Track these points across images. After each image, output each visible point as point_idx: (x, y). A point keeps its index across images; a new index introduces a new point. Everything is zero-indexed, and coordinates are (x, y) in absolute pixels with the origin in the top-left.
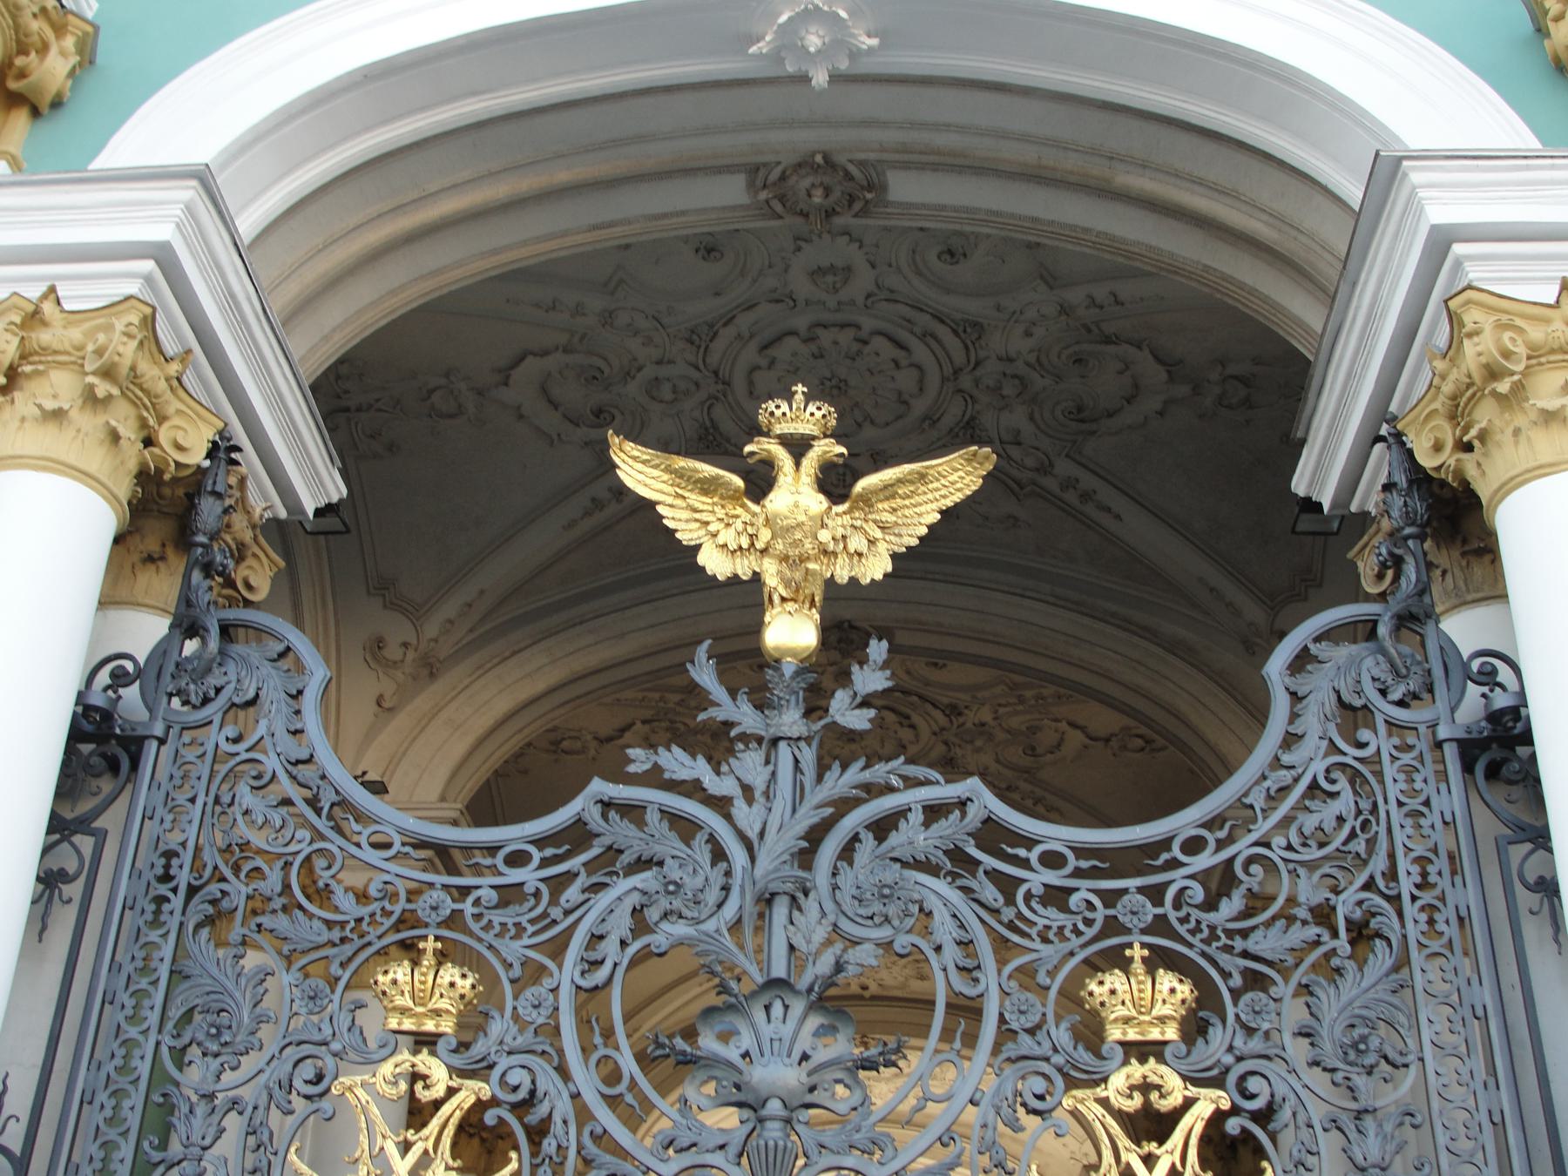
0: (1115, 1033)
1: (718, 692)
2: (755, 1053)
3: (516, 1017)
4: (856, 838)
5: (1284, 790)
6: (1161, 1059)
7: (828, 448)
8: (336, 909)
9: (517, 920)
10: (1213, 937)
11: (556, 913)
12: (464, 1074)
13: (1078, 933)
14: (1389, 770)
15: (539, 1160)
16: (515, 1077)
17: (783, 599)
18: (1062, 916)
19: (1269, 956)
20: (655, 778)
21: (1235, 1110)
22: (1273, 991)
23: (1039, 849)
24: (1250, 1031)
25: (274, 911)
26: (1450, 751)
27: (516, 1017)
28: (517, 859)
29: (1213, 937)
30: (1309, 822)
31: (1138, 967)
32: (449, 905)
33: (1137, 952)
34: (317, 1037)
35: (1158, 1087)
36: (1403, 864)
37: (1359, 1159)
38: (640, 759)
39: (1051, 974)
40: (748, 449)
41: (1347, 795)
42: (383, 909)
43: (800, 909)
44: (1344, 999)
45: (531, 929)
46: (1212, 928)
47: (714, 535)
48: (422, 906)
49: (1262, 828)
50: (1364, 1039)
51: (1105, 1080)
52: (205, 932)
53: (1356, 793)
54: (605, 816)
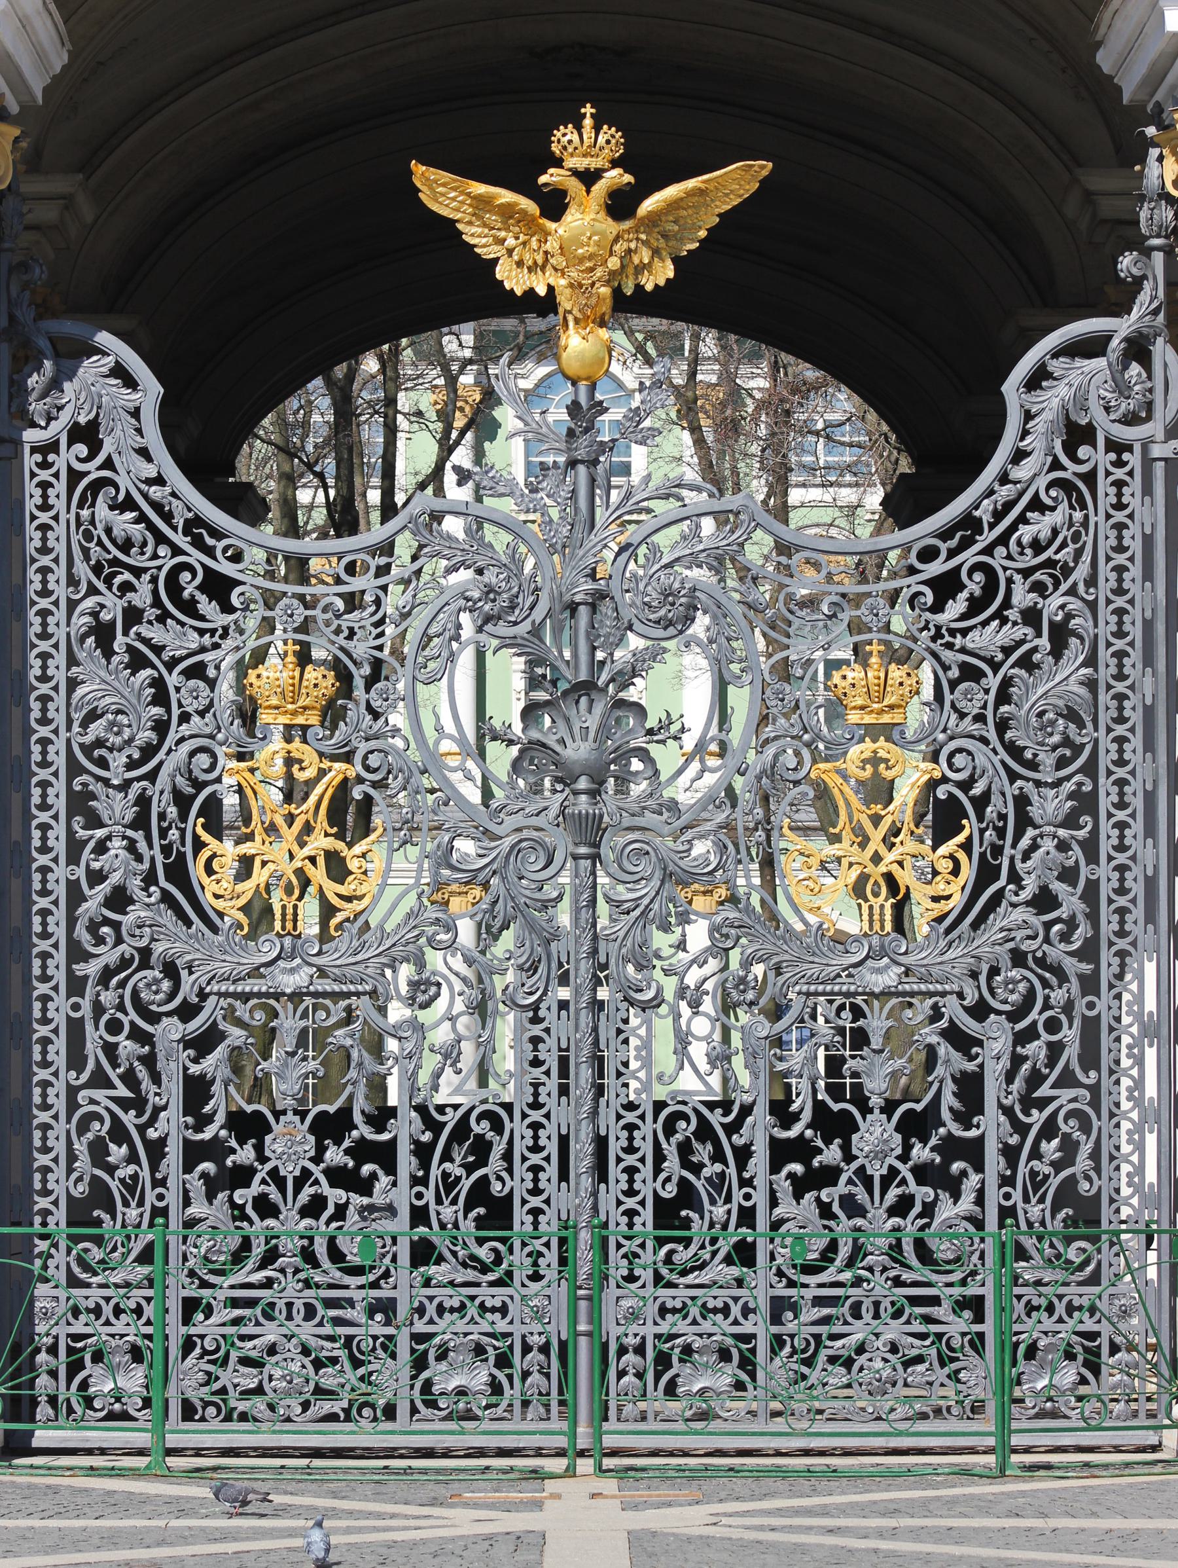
0: (854, 717)
2: (568, 741)
3: (369, 708)
5: (1009, 506)
7: (616, 177)
8: (203, 618)
10: (938, 636)
12: (334, 758)
14: (1102, 484)
16: (374, 761)
21: (945, 780)
22: (984, 681)
24: (962, 716)
26: (1159, 468)
30: (1026, 533)
32: (301, 613)
34: (208, 730)
36: (1104, 570)
37: (1038, 821)
40: (543, 179)
44: (1040, 691)
46: (938, 628)
47: (510, 252)
49: (987, 537)
50: (1052, 723)
52: (90, 641)
53: (1072, 507)
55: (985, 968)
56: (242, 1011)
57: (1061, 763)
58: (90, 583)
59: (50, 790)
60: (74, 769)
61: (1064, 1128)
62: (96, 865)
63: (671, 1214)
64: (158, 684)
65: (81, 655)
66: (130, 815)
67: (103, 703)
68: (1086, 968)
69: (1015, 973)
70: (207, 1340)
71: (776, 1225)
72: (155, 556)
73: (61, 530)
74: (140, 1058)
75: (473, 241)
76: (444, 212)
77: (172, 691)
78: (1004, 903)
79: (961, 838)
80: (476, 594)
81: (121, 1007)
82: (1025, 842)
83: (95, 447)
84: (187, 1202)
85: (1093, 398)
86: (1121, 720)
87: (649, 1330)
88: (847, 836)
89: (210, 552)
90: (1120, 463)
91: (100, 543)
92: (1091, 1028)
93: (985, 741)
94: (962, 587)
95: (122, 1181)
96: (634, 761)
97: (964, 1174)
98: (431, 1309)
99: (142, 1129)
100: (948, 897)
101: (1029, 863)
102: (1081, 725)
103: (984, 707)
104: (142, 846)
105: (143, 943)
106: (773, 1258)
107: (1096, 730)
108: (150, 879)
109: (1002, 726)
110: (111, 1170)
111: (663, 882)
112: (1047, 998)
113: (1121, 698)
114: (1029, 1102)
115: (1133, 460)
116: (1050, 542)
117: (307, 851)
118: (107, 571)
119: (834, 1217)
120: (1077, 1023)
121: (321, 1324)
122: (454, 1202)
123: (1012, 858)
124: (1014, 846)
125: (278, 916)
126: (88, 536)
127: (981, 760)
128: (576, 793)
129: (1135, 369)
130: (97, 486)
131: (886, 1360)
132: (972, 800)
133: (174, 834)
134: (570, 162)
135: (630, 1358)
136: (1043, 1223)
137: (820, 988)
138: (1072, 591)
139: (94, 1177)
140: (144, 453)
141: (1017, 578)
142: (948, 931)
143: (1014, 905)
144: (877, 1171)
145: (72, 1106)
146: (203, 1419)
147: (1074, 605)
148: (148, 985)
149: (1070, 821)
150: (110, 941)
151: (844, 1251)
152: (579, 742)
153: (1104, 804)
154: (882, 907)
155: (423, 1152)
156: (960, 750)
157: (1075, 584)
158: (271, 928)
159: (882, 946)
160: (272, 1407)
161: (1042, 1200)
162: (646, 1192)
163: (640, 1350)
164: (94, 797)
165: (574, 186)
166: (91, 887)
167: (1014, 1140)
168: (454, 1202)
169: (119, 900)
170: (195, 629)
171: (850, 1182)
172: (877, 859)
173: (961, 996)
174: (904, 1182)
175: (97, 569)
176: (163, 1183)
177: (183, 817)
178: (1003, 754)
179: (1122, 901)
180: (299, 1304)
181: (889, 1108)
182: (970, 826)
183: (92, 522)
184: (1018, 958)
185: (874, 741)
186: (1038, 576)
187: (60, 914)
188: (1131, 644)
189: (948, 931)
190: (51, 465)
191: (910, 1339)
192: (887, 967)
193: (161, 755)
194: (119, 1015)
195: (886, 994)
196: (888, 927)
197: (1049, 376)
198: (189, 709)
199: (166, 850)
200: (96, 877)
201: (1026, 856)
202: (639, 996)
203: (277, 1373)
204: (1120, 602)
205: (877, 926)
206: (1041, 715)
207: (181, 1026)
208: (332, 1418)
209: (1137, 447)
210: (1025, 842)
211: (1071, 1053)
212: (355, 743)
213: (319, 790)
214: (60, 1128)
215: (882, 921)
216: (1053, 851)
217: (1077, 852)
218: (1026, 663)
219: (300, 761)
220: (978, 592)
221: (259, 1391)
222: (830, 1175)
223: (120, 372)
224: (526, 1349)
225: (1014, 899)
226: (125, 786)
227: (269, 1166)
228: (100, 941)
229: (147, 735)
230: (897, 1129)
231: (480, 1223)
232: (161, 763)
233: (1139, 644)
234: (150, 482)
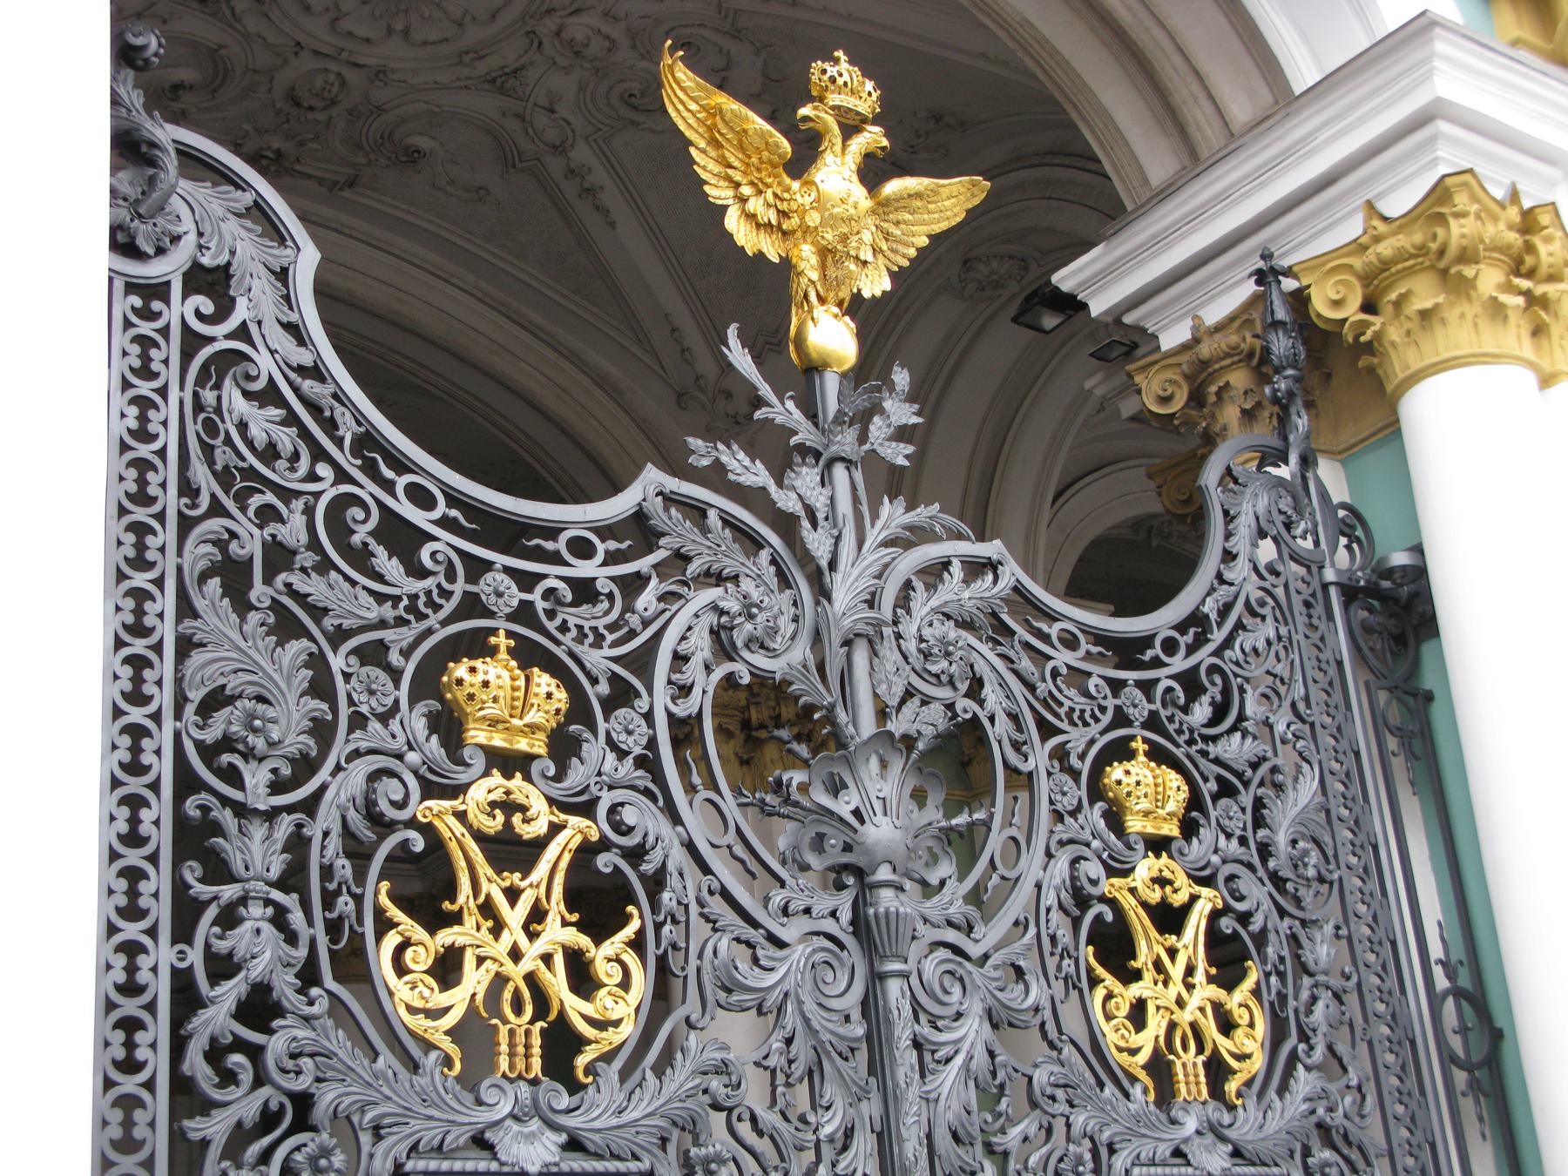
1: (765, 390)
3: (610, 742)
4: (908, 585)
7: (873, 137)
8: (380, 578)
9: (594, 623)
11: (634, 621)
13: (1097, 720)
15: (661, 918)
18: (1083, 700)
19: (1235, 766)
20: (716, 477)
21: (1227, 909)
23: (1058, 626)
25: (303, 570)
27: (610, 742)
28: (582, 549)
32: (515, 596)
33: (1139, 746)
37: (1312, 966)
38: (701, 452)
39: (1082, 757)
43: (876, 654)
45: (610, 638)
48: (484, 587)
49: (1218, 636)
50: (1306, 853)
51: (1132, 869)
52: (214, 584)
53: (1276, 620)
54: (666, 509)
55: (1298, 1147)
60: (186, 783)
62: (221, 946)
64: (317, 662)
65: (200, 604)
72: (313, 477)
75: (704, 176)
77: (339, 679)
78: (1300, 1067)
80: (733, 605)
82: (1305, 995)
83: (225, 308)
88: (1149, 975)
89: (389, 486)
91: (228, 441)
103: (1244, 829)
104: (297, 918)
105: (302, 1084)
108: (309, 976)
117: (541, 945)
123: (1296, 1011)
126: (211, 428)
133: (345, 904)
134: (834, 99)
140: (295, 331)
150: (246, 1077)
158: (494, 1066)
164: (218, 829)
169: (259, 1009)
170: (371, 592)
172: (1180, 1003)
175: (224, 477)
177: (360, 875)
178: (1270, 887)
183: (218, 410)
185: (1158, 856)
187: (160, 1028)
193: (323, 775)
198: (364, 709)
199: (334, 928)
201: (1309, 1012)
205: (1193, 1088)
212: (594, 789)
219: (523, 809)
220: (1218, 698)
223: (259, 212)
225: (1309, 1061)
228: (228, 1078)
229: (298, 742)
232: (323, 788)
234: (301, 370)
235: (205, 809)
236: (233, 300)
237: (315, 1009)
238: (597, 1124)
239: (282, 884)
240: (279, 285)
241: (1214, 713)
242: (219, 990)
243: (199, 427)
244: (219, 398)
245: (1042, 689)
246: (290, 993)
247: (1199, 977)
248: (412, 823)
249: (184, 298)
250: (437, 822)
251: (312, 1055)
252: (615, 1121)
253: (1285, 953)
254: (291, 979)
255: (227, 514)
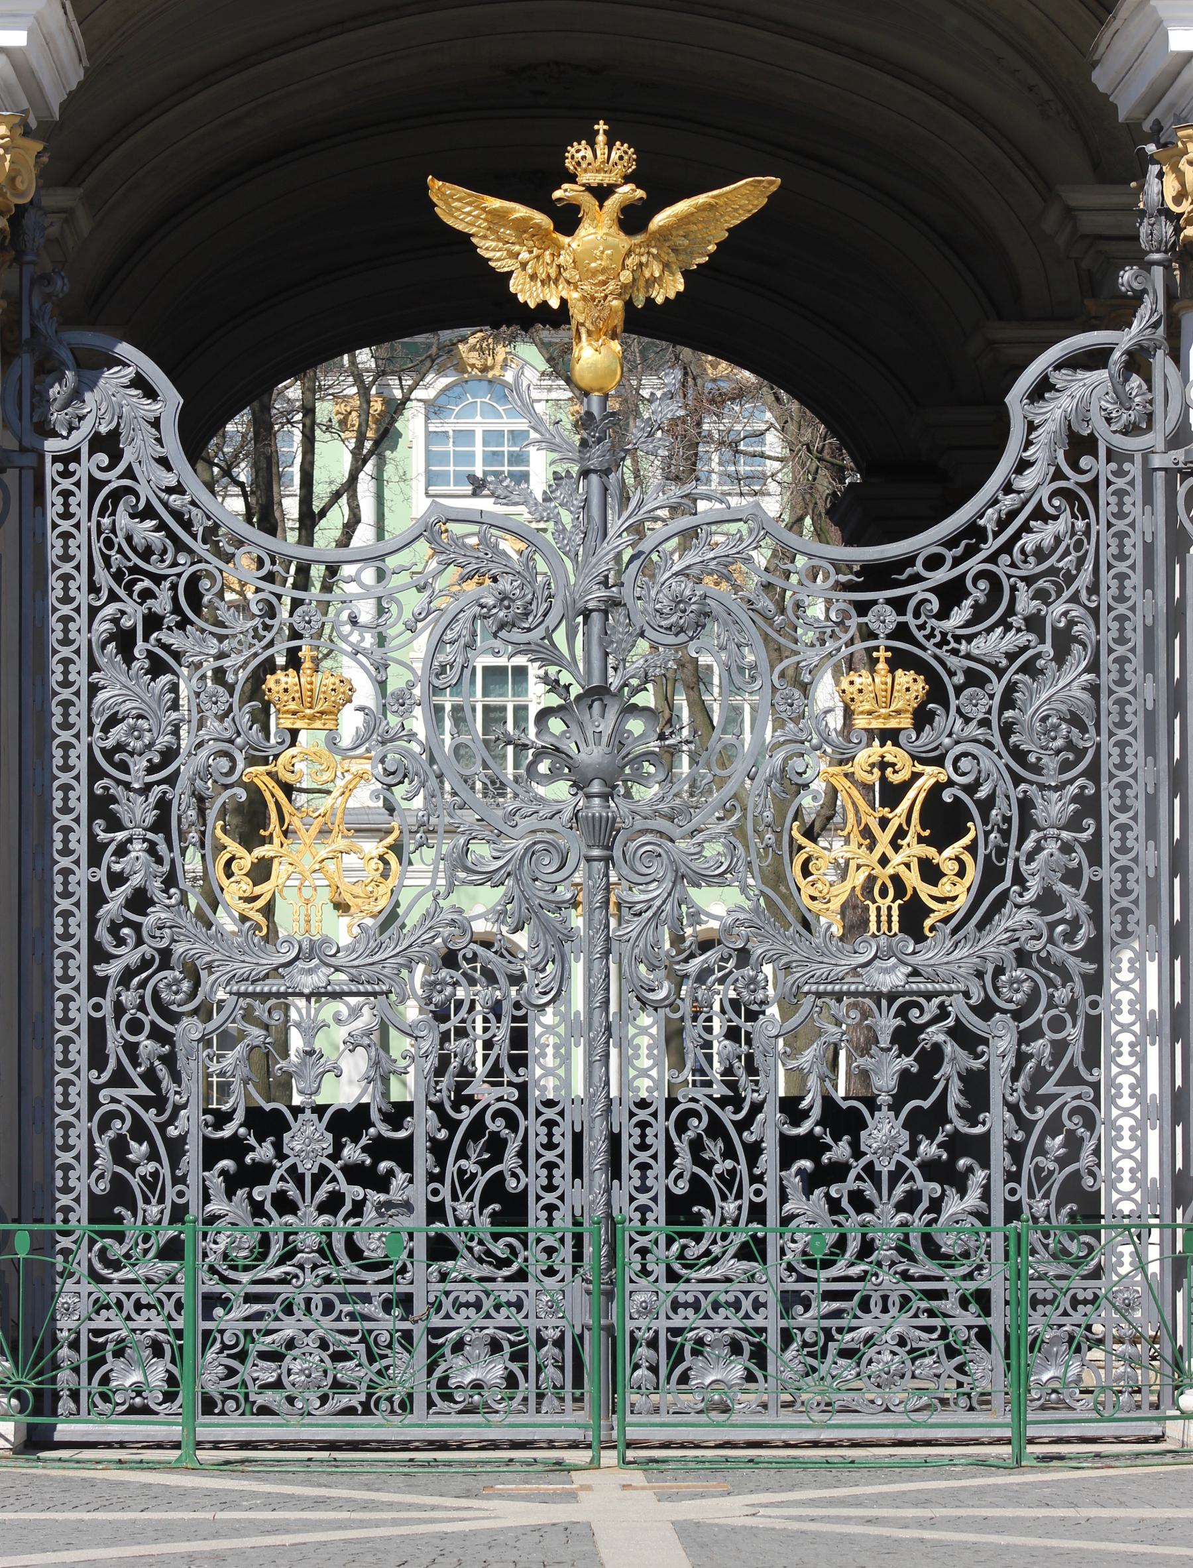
5: (1013, 514)
6: (896, 744)
7: (628, 192)
10: (944, 642)
14: (1103, 493)
17: (589, 333)
19: (987, 659)
21: (950, 783)
22: (988, 687)
29: (944, 642)
30: (1029, 541)
31: (882, 666)
34: (227, 735)
35: (893, 765)
36: (1105, 577)
40: (557, 194)
41: (1066, 517)
42: (264, 623)
44: (1044, 696)
46: (944, 635)
47: (524, 265)
50: (1056, 727)
52: (111, 647)
53: (1074, 516)
55: (990, 968)
56: (260, 1010)
57: (1065, 766)
58: (111, 591)
59: (71, 794)
60: (95, 772)
61: (1069, 1125)
62: (117, 868)
63: (681, 1210)
65: (102, 661)
66: (150, 818)
67: (123, 708)
68: (1090, 967)
69: (1019, 973)
70: (227, 1335)
71: (785, 1221)
72: (175, 564)
73: (82, 538)
74: (160, 1058)
75: (487, 255)
76: (459, 226)
78: (1009, 904)
79: (966, 841)
80: (490, 601)
81: (142, 1007)
84: (207, 1199)
85: (1094, 409)
86: (1122, 724)
87: (662, 1324)
88: (856, 838)
90: (1120, 473)
91: (121, 551)
92: (1093, 1028)
93: (990, 745)
94: (968, 594)
95: (143, 1178)
96: (646, 764)
97: (970, 1169)
98: (447, 1304)
99: (162, 1127)
100: (954, 898)
101: (1033, 865)
102: (1084, 729)
103: (989, 712)
104: (162, 848)
105: (163, 944)
106: (783, 1253)
107: (1098, 734)
109: (1007, 730)
110: (708, 1165)
111: (674, 883)
112: (1051, 997)
113: (1122, 703)
114: (1033, 1099)
115: (1135, 469)
116: (1054, 549)
118: (127, 578)
119: (844, 1212)
120: (1081, 1021)
121: (338, 1319)
122: (470, 1198)
123: (1017, 860)
124: (1018, 848)
125: (873, 918)
126: (109, 544)
127: (986, 764)
128: (589, 796)
129: (1136, 381)
130: (116, 496)
131: (894, 1353)
132: (978, 803)
134: (584, 178)
135: (643, 1351)
136: (1047, 1218)
137: (829, 987)
138: (1075, 599)
139: (115, 1174)
141: (1021, 585)
142: (954, 931)
143: (1019, 907)
144: (885, 1167)
145: (94, 1104)
146: (222, 1413)
147: (1077, 612)
148: (169, 986)
149: (1074, 824)
150: (131, 942)
151: (853, 1246)
152: (592, 746)
153: (1106, 807)
154: (889, 908)
155: (439, 1150)
156: (965, 754)
157: (1077, 591)
159: (890, 947)
160: (291, 1400)
161: (1046, 1196)
162: (659, 1188)
163: (653, 1344)
164: (114, 800)
165: (588, 202)
166: (112, 889)
167: (1019, 1137)
168: (470, 1198)
169: (140, 901)
171: (859, 1178)
172: (884, 861)
173: (967, 995)
174: (911, 1178)
175: (118, 576)
176: (182, 1180)
179: (1124, 902)
180: (317, 1300)
181: (896, 1107)
182: (974, 829)
183: (113, 531)
184: (1022, 958)
186: (1041, 583)
187: (82, 915)
188: (1133, 650)
189: (954, 931)
190: (73, 474)
191: (918, 1333)
192: (894, 967)
194: (140, 1015)
195: (892, 997)
196: (895, 927)
197: (1052, 388)
200: (117, 879)
201: (1030, 858)
202: (651, 996)
203: (296, 1366)
204: (1121, 609)
205: (884, 927)
206: (1044, 719)
207: (201, 1026)
208: (349, 1411)
209: (1138, 458)
210: (1029, 845)
211: (1076, 1050)
213: (911, 794)
214: (82, 1126)
215: (890, 922)
216: (1056, 853)
217: (1080, 856)
218: (1029, 668)
220: (982, 600)
221: (278, 1385)
222: (838, 1172)
224: (541, 1343)
225: (1019, 900)
226: (146, 789)
227: (287, 1163)
228: (121, 942)
230: (904, 1127)
231: (495, 1218)
233: (1140, 650)
234: (170, 490)
235: (106, 788)
236: (122, 450)
237: (173, 901)
238: (356, 963)
239: (154, 828)
240: (153, 431)
241: (973, 614)
242: (115, 893)
243: (101, 544)
244: (114, 522)
245: (778, 619)
246: (157, 892)
247: (910, 838)
248: (239, 783)
249: (91, 455)
250: (256, 780)
251: (171, 927)
252: (370, 960)
253: (1015, 814)
254: (158, 884)
255: (120, 600)
